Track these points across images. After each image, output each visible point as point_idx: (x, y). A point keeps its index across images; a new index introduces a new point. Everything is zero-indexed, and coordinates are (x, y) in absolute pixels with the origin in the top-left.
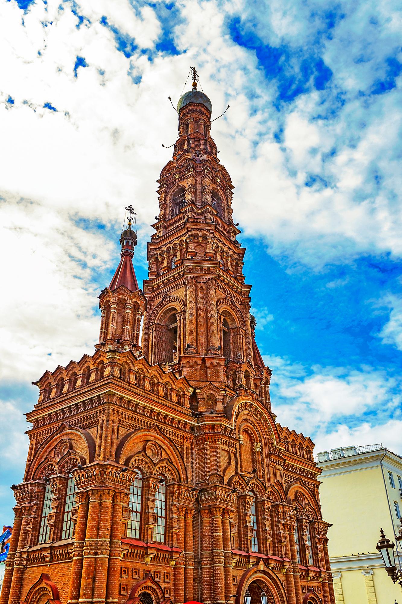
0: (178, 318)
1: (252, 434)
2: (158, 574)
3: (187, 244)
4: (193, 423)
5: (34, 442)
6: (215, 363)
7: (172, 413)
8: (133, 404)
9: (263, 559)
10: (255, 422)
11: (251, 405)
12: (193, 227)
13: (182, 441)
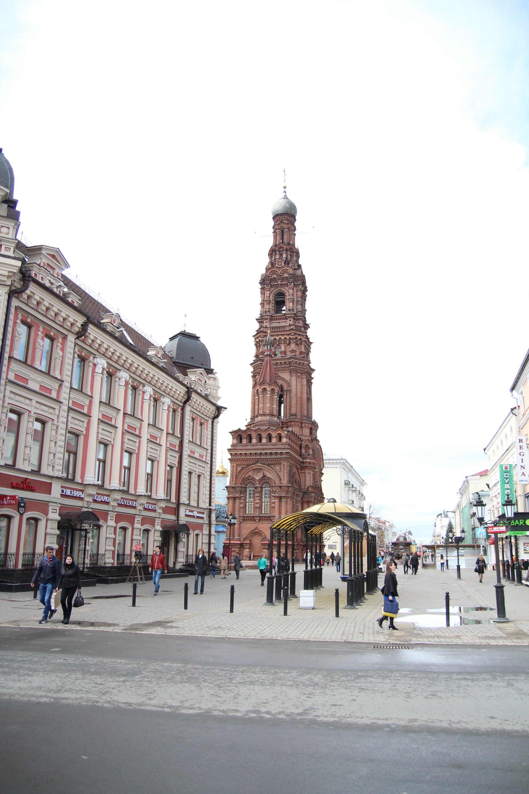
0: (285, 393)
3: (290, 343)
5: (235, 465)
6: (307, 425)
12: (296, 332)
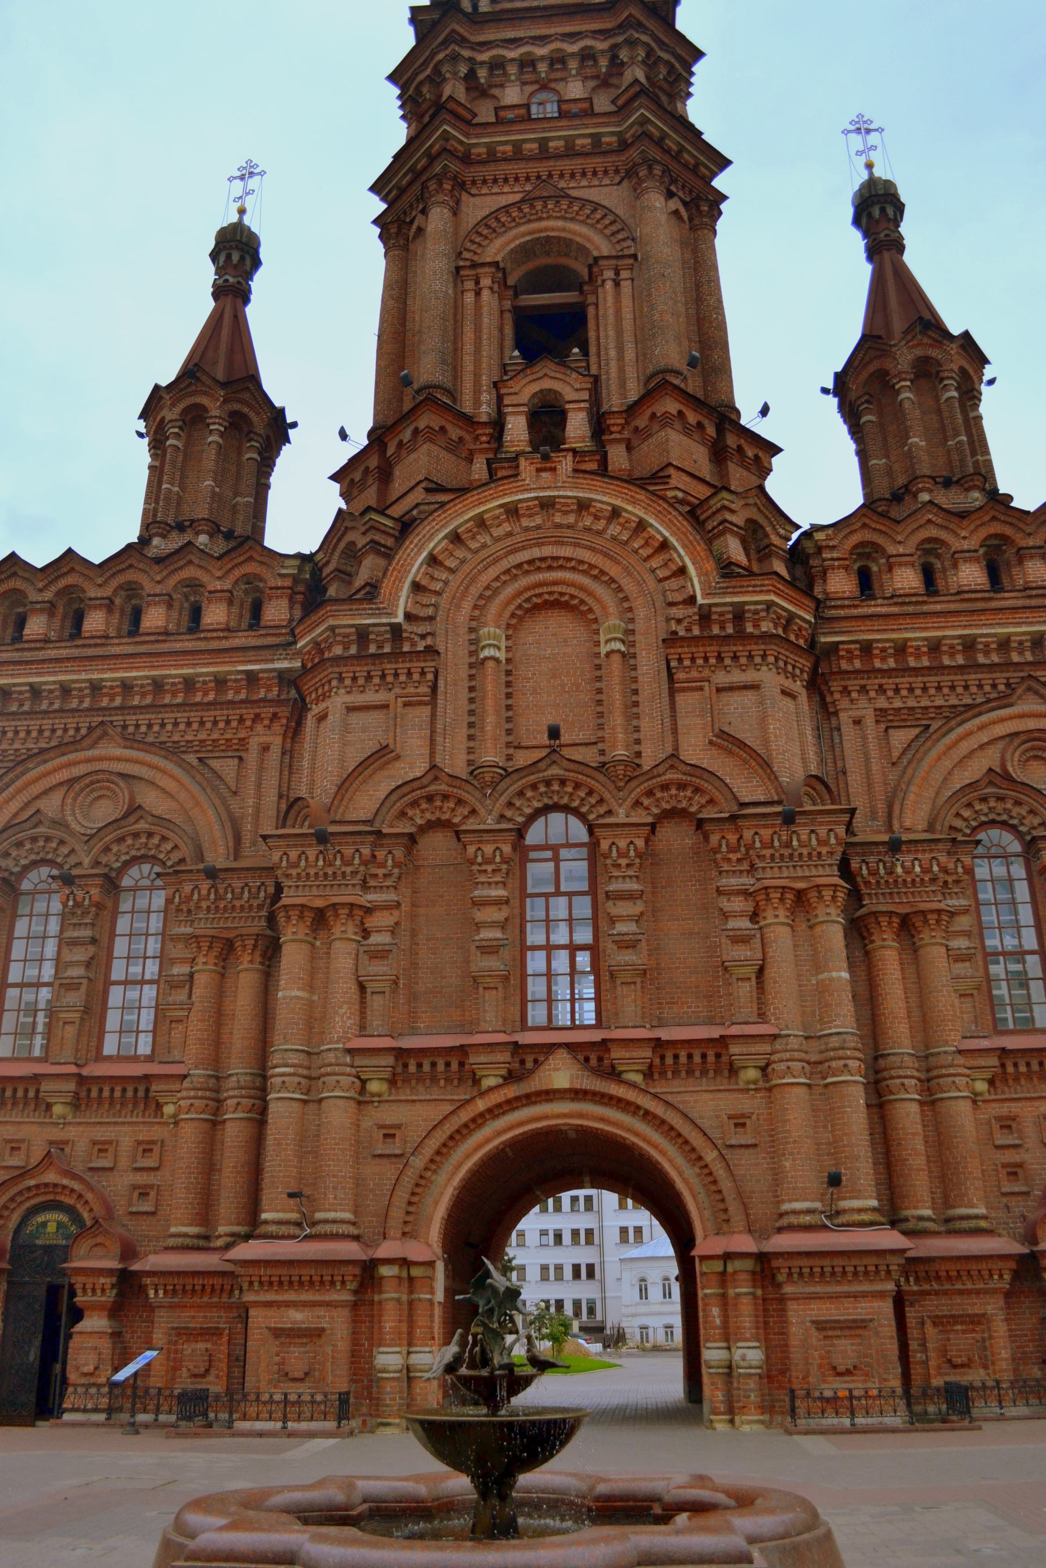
1: (582, 602)
2: (102, 1147)
4: (285, 665)
6: (407, 435)
7: (182, 666)
8: (20, 693)
9: (571, 1047)
10: (586, 555)
11: (547, 505)
13: (242, 734)
